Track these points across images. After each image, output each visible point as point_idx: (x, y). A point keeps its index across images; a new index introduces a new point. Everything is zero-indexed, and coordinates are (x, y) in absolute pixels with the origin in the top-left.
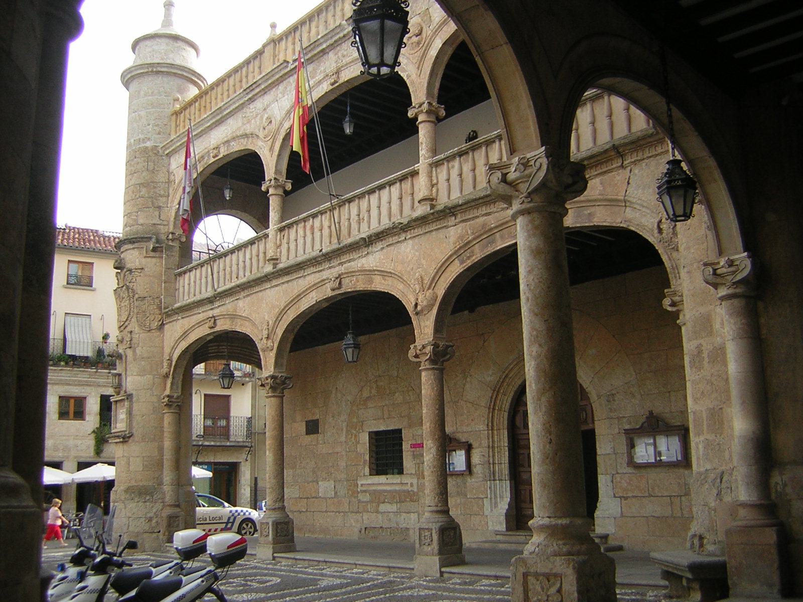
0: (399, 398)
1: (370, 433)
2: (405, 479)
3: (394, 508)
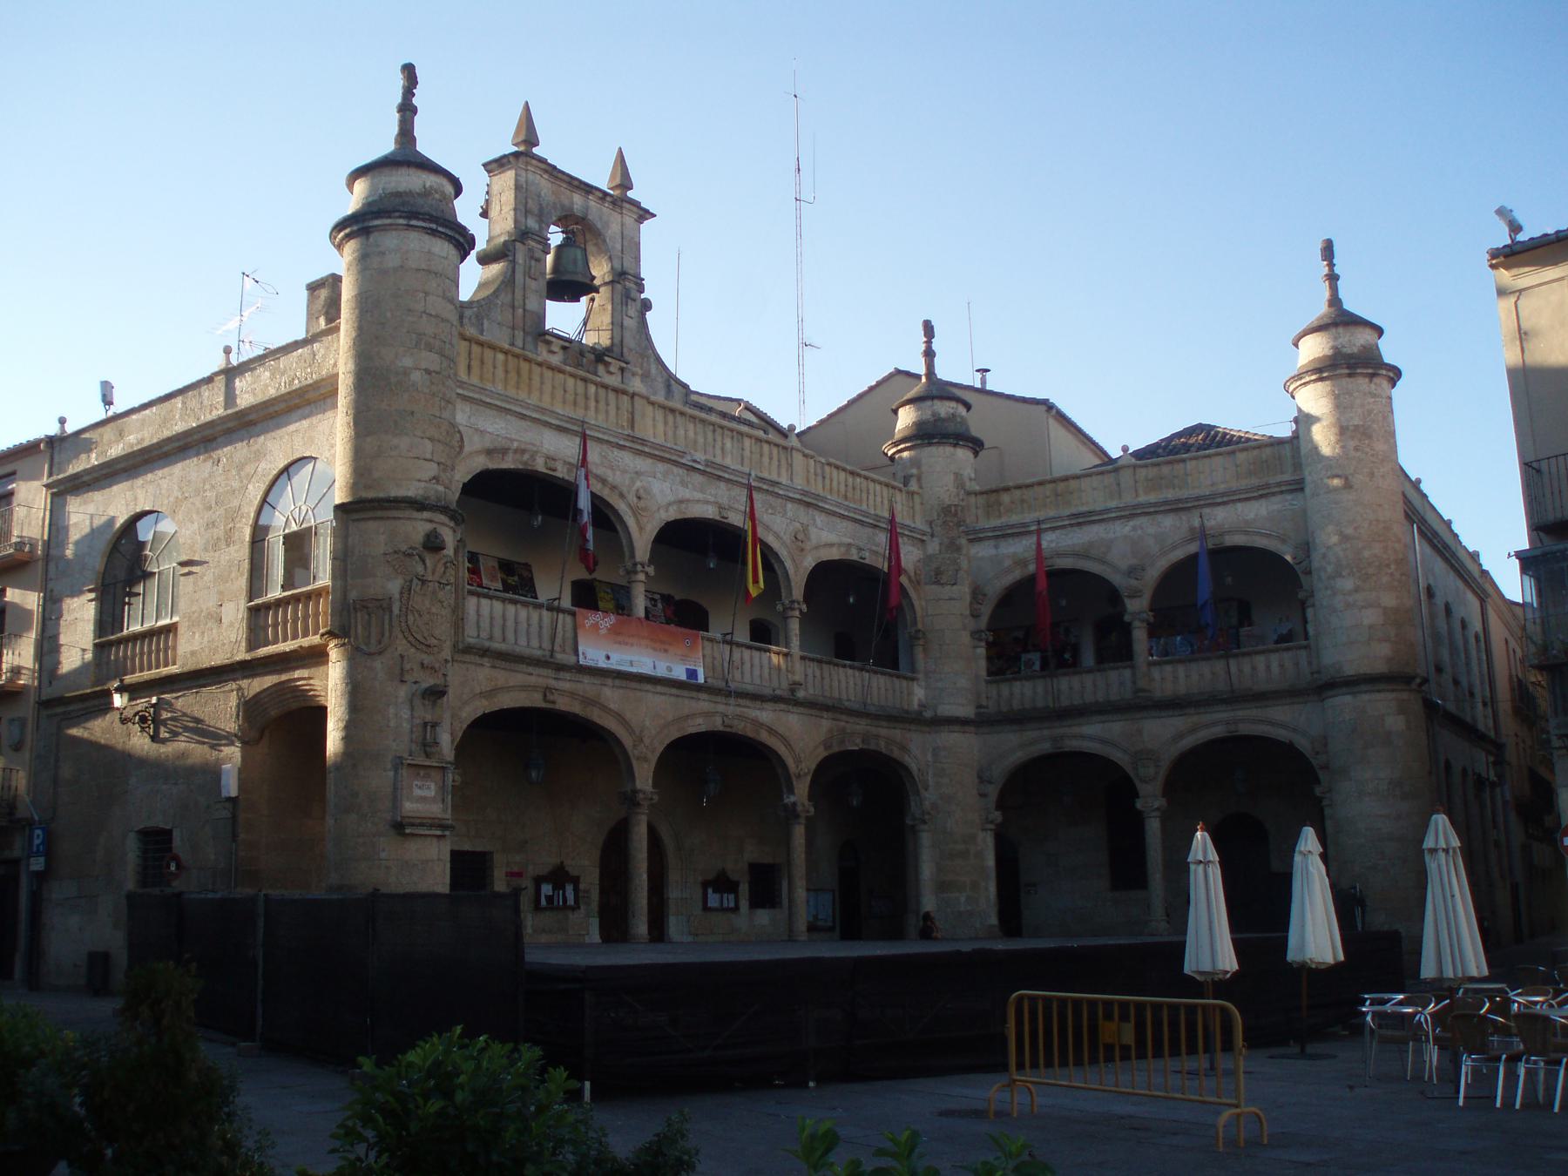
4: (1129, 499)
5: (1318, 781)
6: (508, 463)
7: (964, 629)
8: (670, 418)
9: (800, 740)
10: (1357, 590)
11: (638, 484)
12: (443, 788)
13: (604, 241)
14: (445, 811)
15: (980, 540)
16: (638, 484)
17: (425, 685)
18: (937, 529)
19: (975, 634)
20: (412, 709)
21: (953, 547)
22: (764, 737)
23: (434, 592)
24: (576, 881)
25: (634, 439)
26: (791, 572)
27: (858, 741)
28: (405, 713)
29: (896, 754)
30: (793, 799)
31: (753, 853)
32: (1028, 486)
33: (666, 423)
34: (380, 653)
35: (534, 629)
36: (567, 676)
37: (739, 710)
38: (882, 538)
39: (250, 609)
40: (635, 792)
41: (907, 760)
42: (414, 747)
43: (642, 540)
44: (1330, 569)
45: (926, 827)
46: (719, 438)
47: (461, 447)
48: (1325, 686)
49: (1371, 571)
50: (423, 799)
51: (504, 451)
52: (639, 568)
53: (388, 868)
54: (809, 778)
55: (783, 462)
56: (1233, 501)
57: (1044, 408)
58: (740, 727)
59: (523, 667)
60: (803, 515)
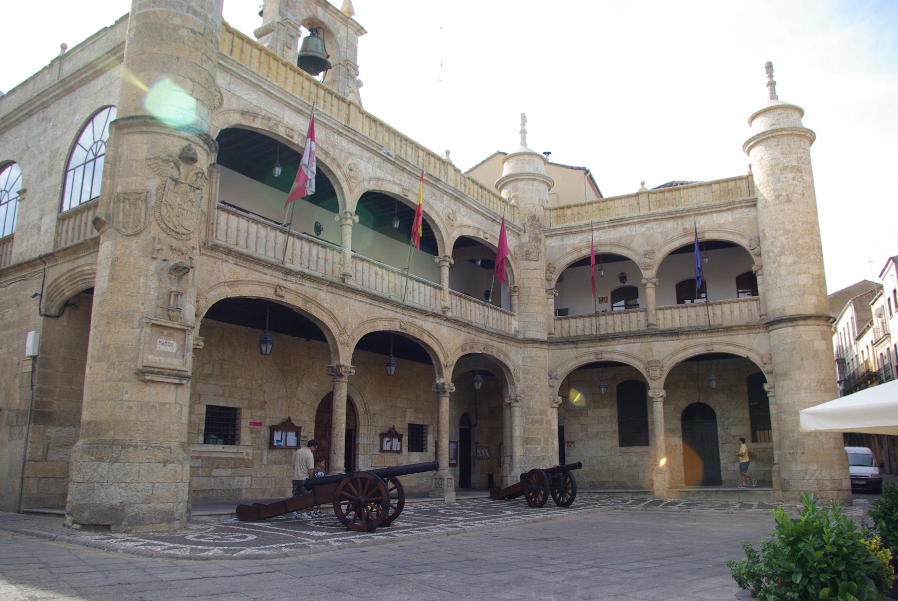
0: (241, 382)
1: (209, 407)
2: (241, 449)
3: (229, 472)
4: (645, 211)
5: (766, 382)
6: (257, 124)
7: (542, 287)
8: (373, 125)
9: (448, 345)
10: (795, 263)
11: (350, 161)
12: (183, 347)
13: (336, 41)
14: (184, 365)
15: (552, 236)
16: (350, 161)
17: (172, 263)
18: (528, 229)
19: (548, 291)
20: (160, 280)
21: (537, 239)
22: (426, 339)
23: (186, 193)
24: (298, 431)
25: (350, 130)
26: (445, 238)
27: (482, 348)
28: (154, 284)
29: (502, 358)
30: (442, 381)
31: (412, 418)
32: (582, 205)
33: (370, 128)
34: (136, 235)
35: (271, 244)
36: (293, 279)
37: (410, 319)
38: (498, 229)
39: (59, 219)
40: (340, 366)
41: (508, 363)
42: (159, 311)
43: (350, 199)
44: (776, 251)
45: (517, 404)
46: (404, 146)
47: (221, 104)
48: (771, 324)
49: (804, 252)
50: (166, 354)
51: (255, 116)
52: (349, 215)
53: (130, 407)
54: (452, 368)
55: (442, 171)
56: (711, 212)
57: (584, 172)
58: (412, 331)
59: (260, 268)
60: (454, 206)
